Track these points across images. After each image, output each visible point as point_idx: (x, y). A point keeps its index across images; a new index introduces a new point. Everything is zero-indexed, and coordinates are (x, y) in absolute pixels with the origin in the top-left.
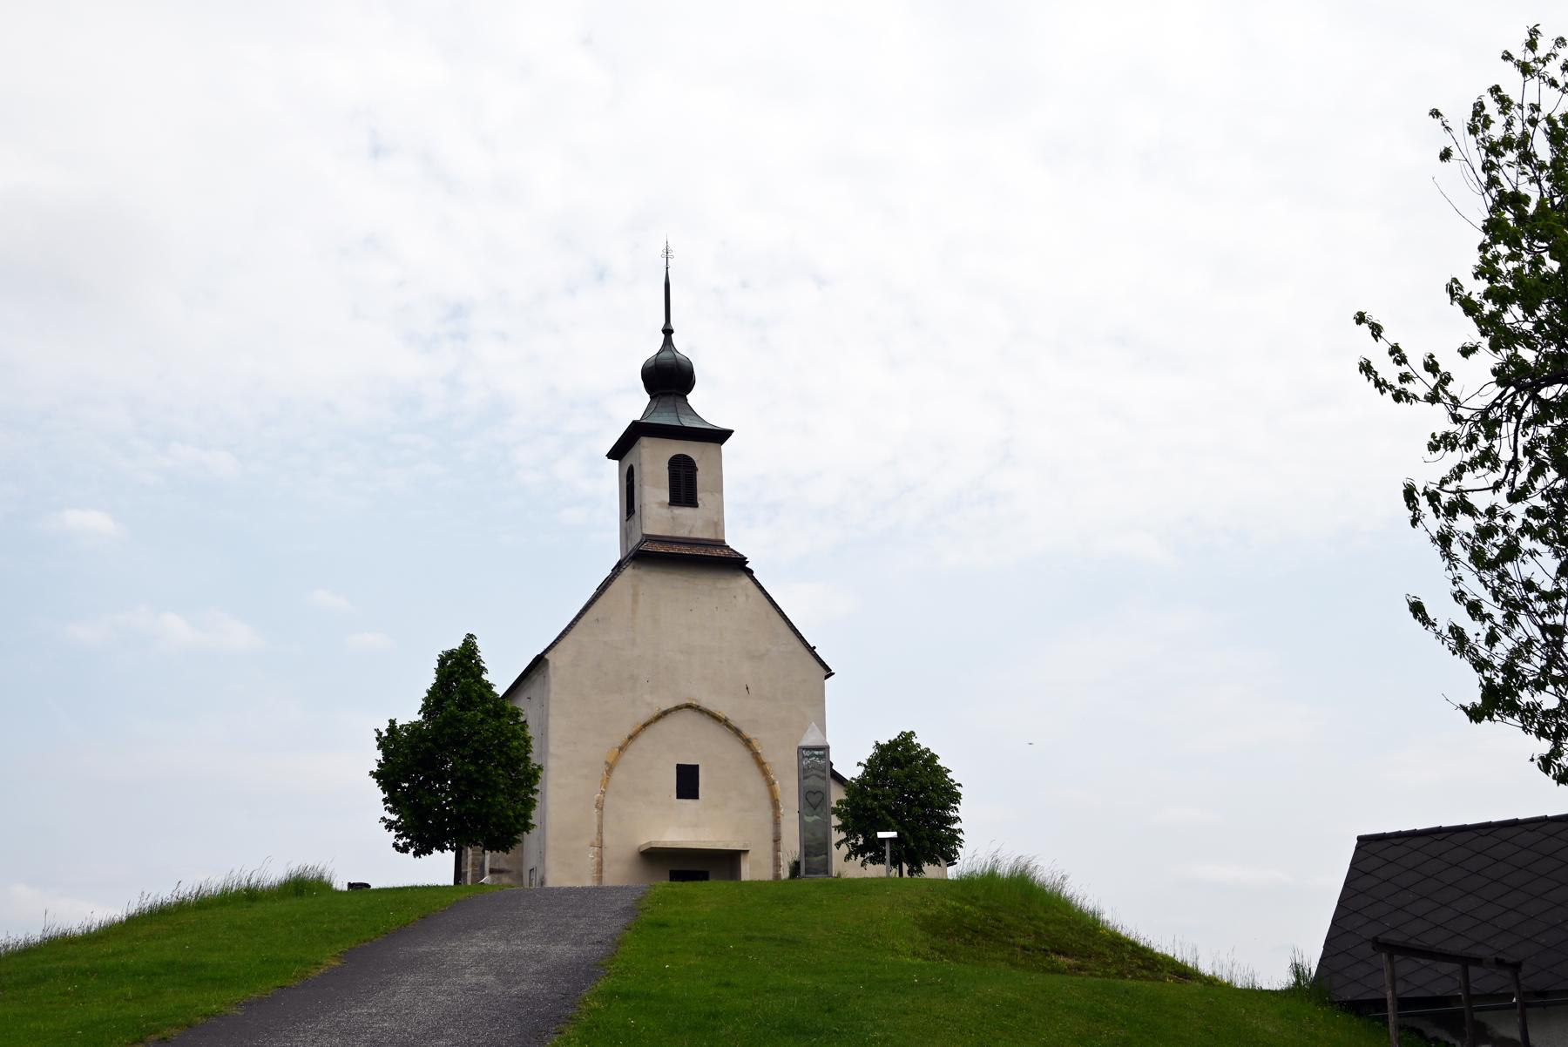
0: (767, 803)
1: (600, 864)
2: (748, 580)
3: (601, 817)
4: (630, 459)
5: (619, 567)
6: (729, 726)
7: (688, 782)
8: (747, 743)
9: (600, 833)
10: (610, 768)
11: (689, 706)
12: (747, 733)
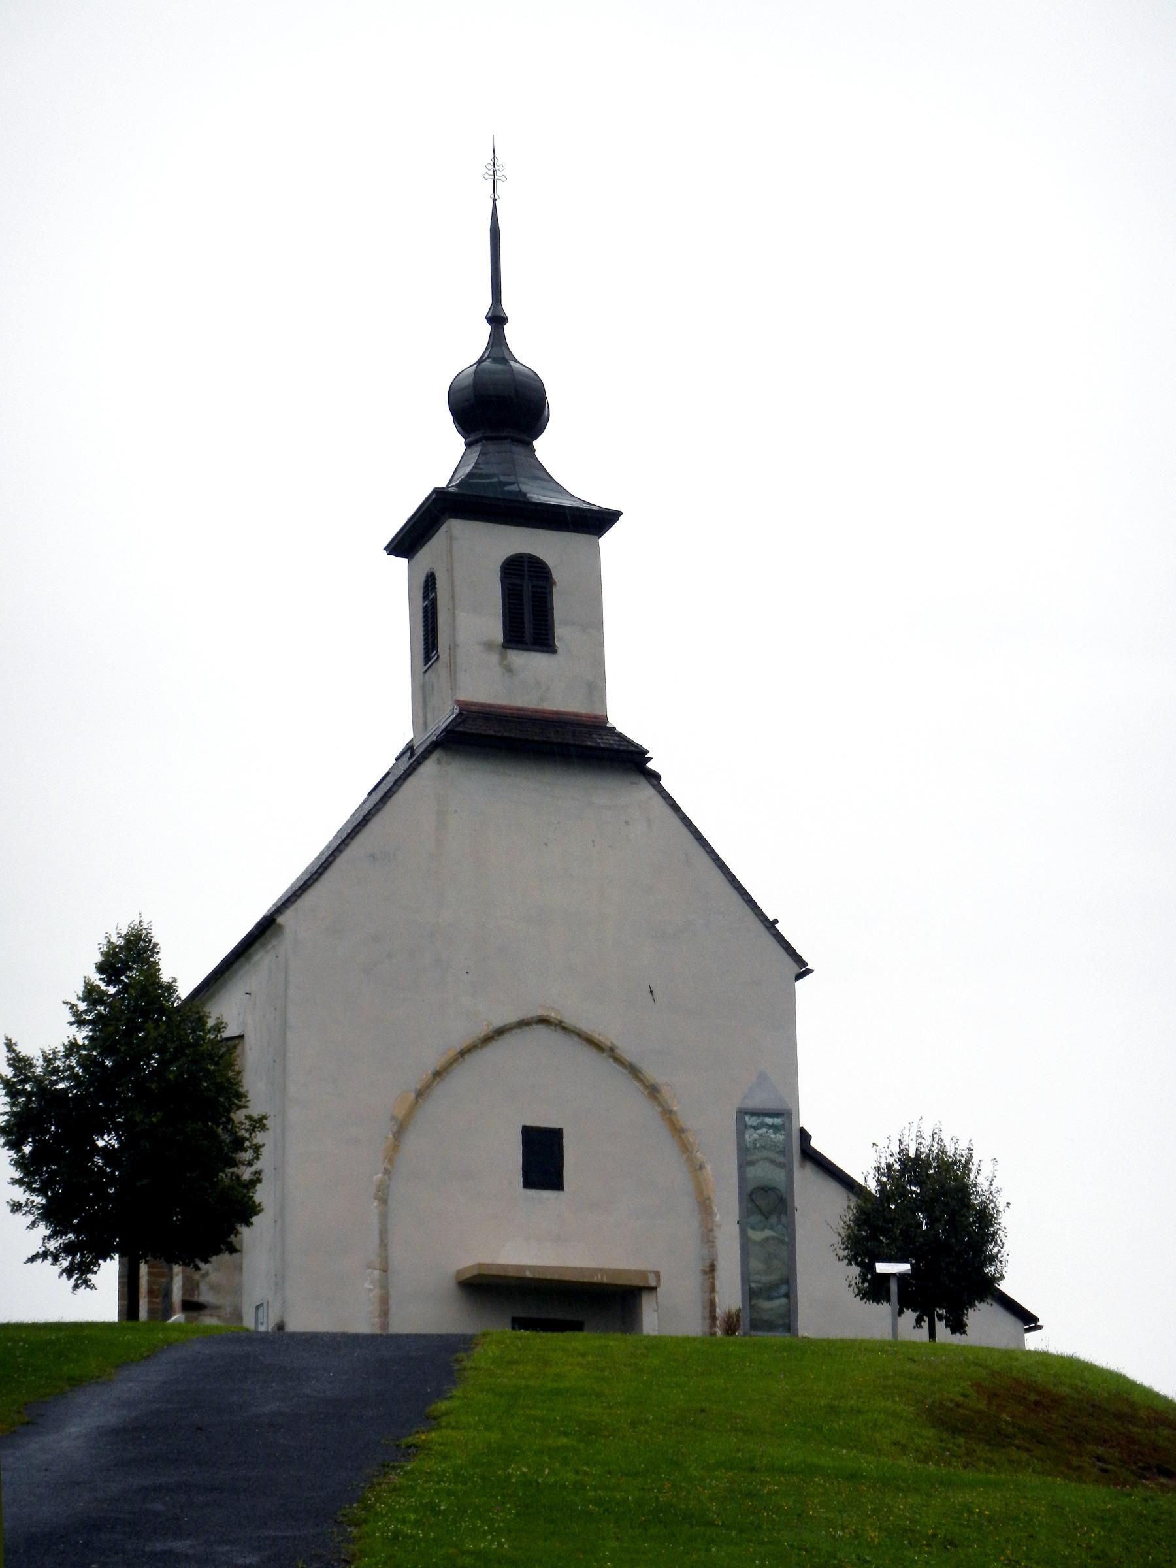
1: (384, 1300)
2: (651, 791)
4: (431, 552)
5: (412, 759)
6: (618, 1060)
7: (543, 1158)
8: (653, 1091)
9: (384, 1244)
10: (401, 1130)
11: (544, 1021)
12: (652, 1073)
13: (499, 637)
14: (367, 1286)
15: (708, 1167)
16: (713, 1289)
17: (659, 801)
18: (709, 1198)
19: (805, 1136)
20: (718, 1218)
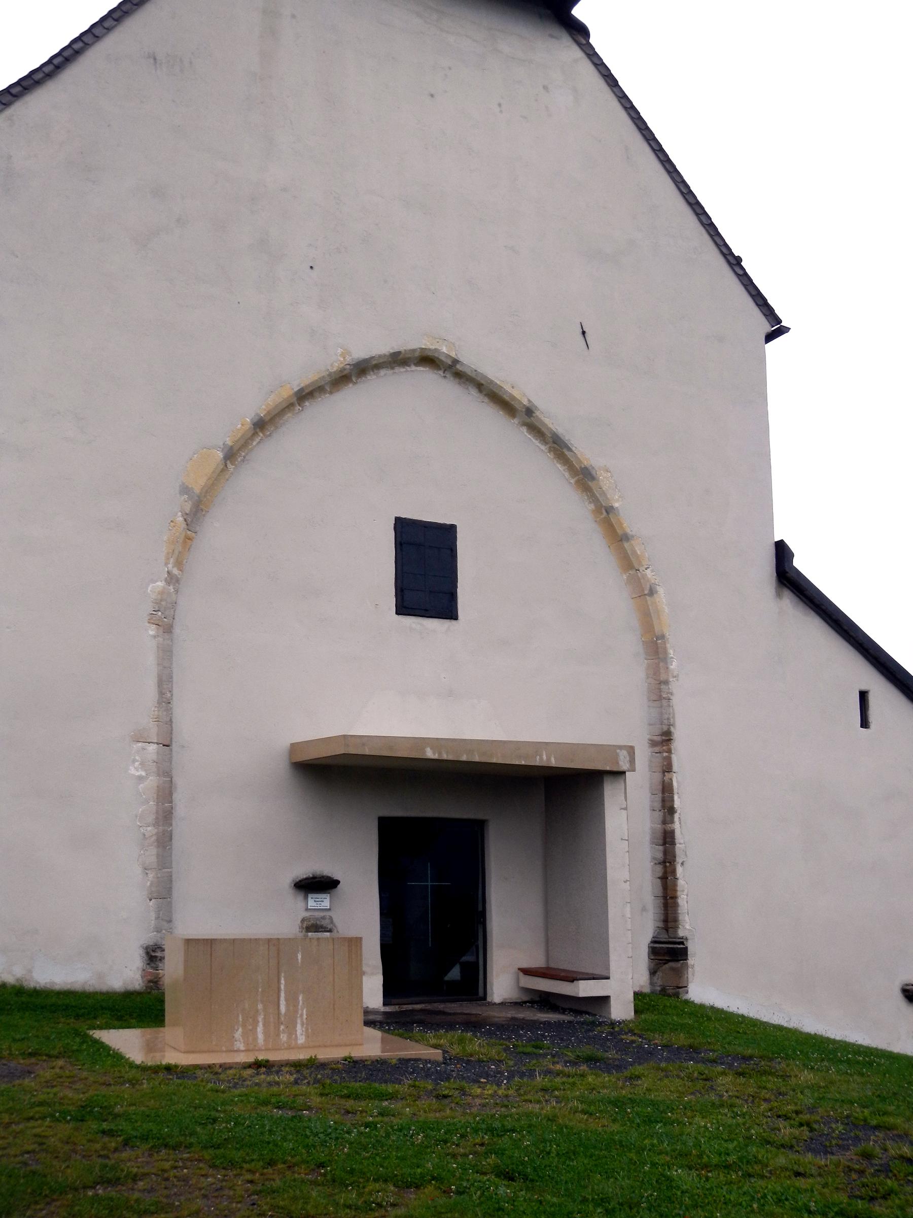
0: (630, 644)
1: (166, 795)
2: (576, 53)
3: (166, 655)
7: (426, 572)
8: (584, 478)
9: (165, 700)
10: (198, 509)
11: (428, 360)
12: (586, 450)
15: (661, 590)
16: (667, 768)
18: (663, 637)
19: (782, 552)
20: (674, 666)
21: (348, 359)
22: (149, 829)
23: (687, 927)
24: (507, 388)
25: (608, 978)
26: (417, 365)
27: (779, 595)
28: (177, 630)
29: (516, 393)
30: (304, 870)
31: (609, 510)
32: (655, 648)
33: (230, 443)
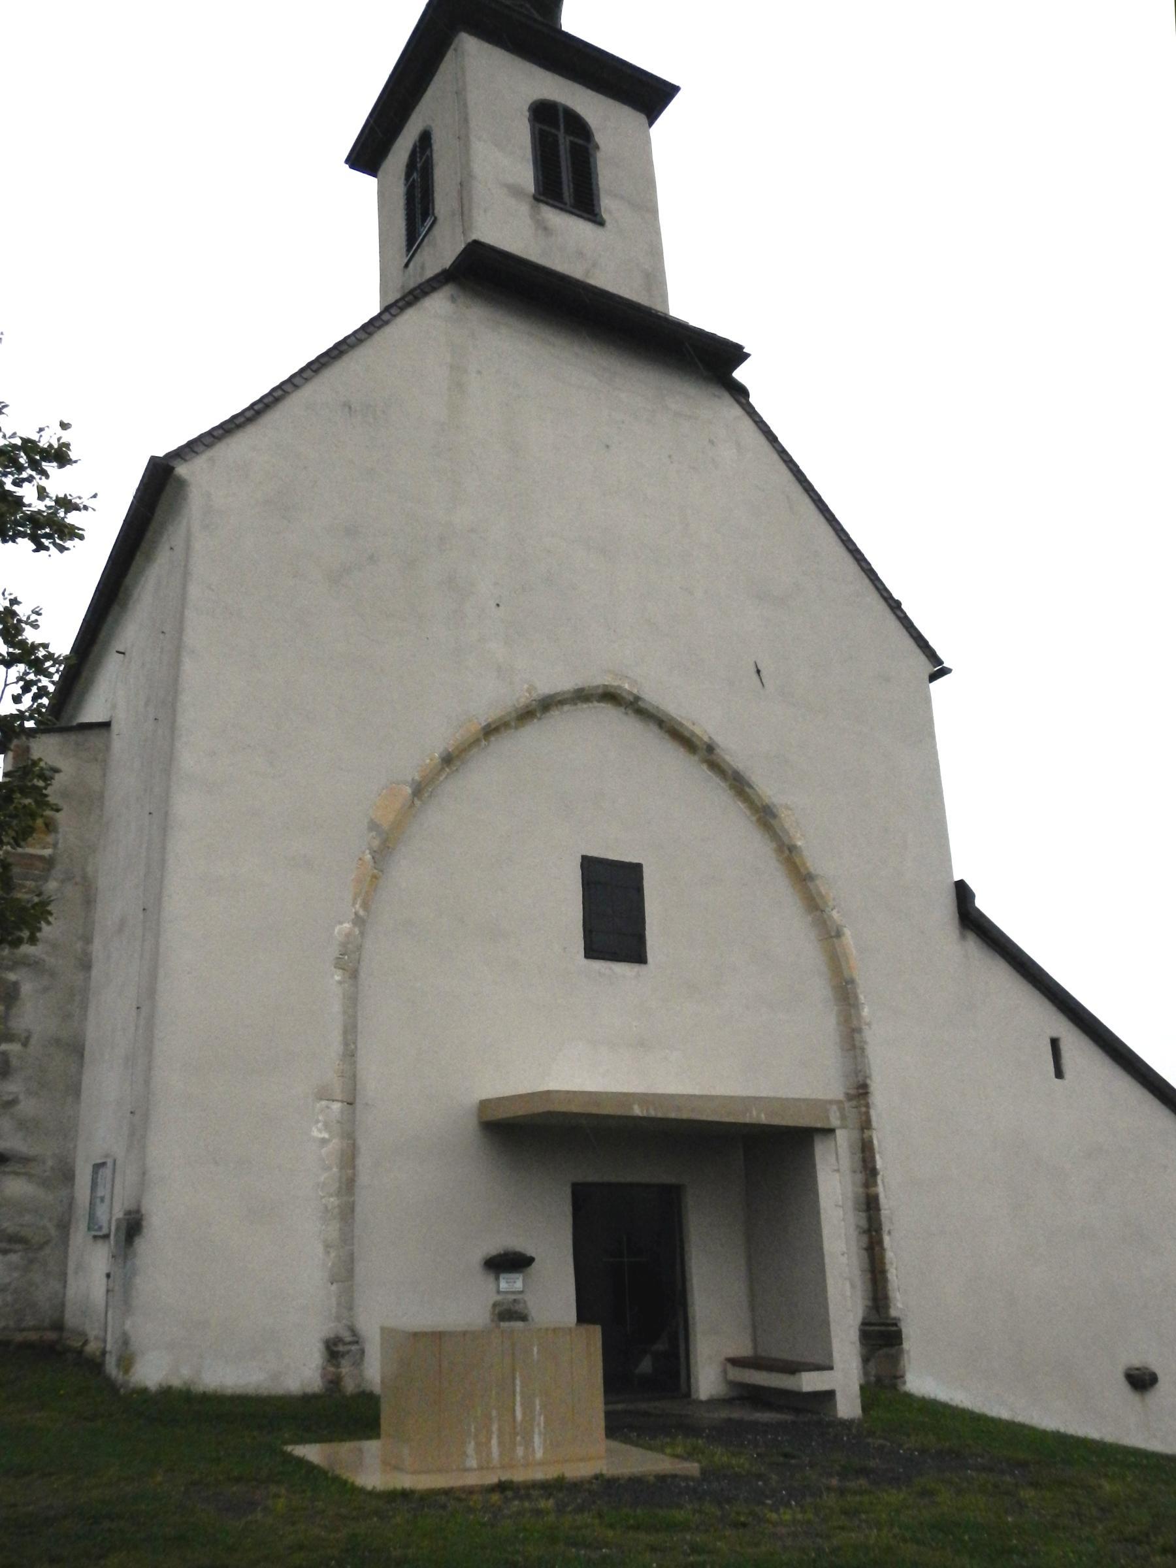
0: (819, 990)
1: (349, 1158)
2: (737, 411)
3: (352, 1002)
8: (765, 816)
9: (350, 1054)
10: (386, 844)
11: (610, 696)
12: (767, 788)
13: (531, 187)
14: (317, 1133)
15: (847, 932)
17: (747, 423)
18: (852, 981)
19: (963, 892)
20: (866, 1012)
21: (534, 695)
22: (332, 1199)
23: (900, 1304)
24: (688, 724)
25: (831, 1368)
26: (599, 701)
27: (963, 937)
28: (362, 975)
29: (698, 731)
30: (494, 1245)
31: (792, 849)
32: (845, 994)
33: (417, 778)
